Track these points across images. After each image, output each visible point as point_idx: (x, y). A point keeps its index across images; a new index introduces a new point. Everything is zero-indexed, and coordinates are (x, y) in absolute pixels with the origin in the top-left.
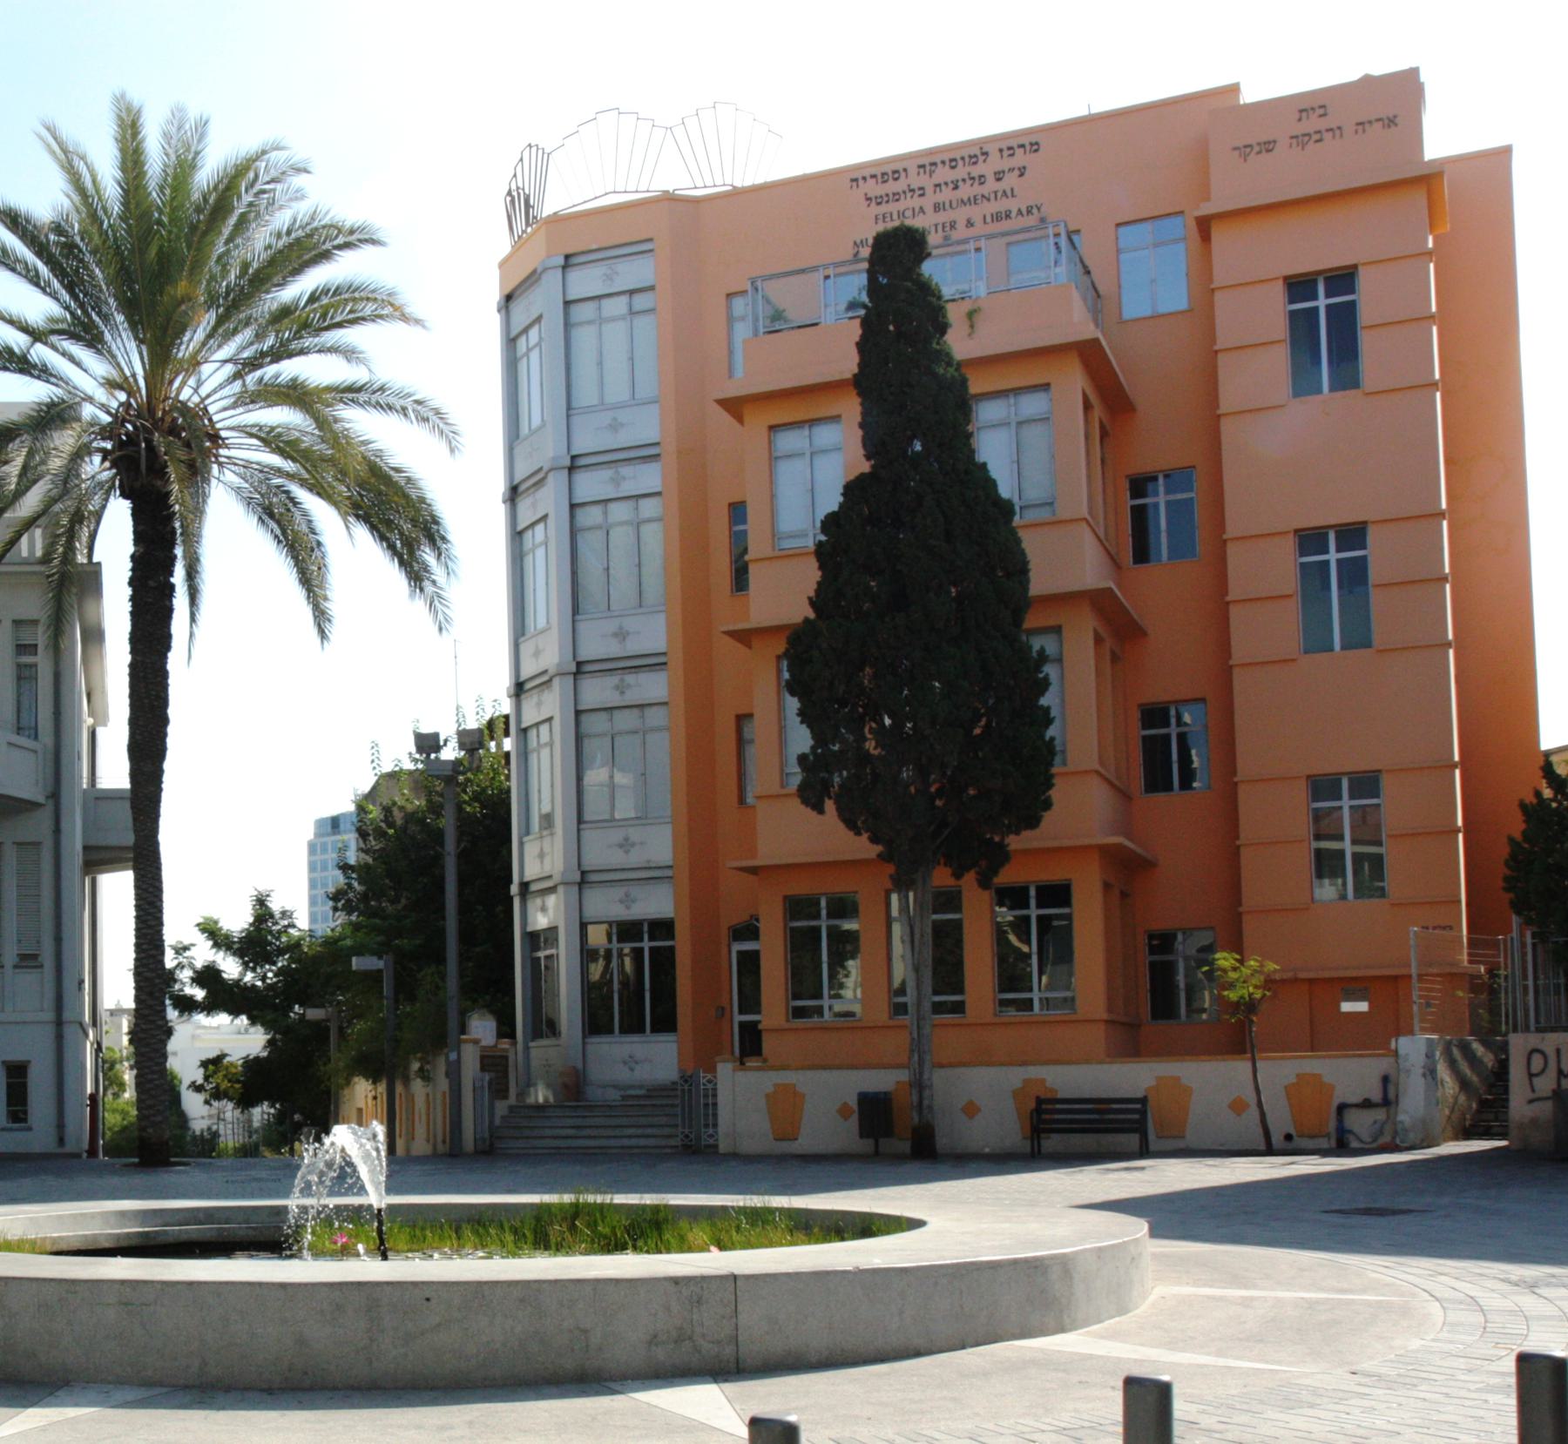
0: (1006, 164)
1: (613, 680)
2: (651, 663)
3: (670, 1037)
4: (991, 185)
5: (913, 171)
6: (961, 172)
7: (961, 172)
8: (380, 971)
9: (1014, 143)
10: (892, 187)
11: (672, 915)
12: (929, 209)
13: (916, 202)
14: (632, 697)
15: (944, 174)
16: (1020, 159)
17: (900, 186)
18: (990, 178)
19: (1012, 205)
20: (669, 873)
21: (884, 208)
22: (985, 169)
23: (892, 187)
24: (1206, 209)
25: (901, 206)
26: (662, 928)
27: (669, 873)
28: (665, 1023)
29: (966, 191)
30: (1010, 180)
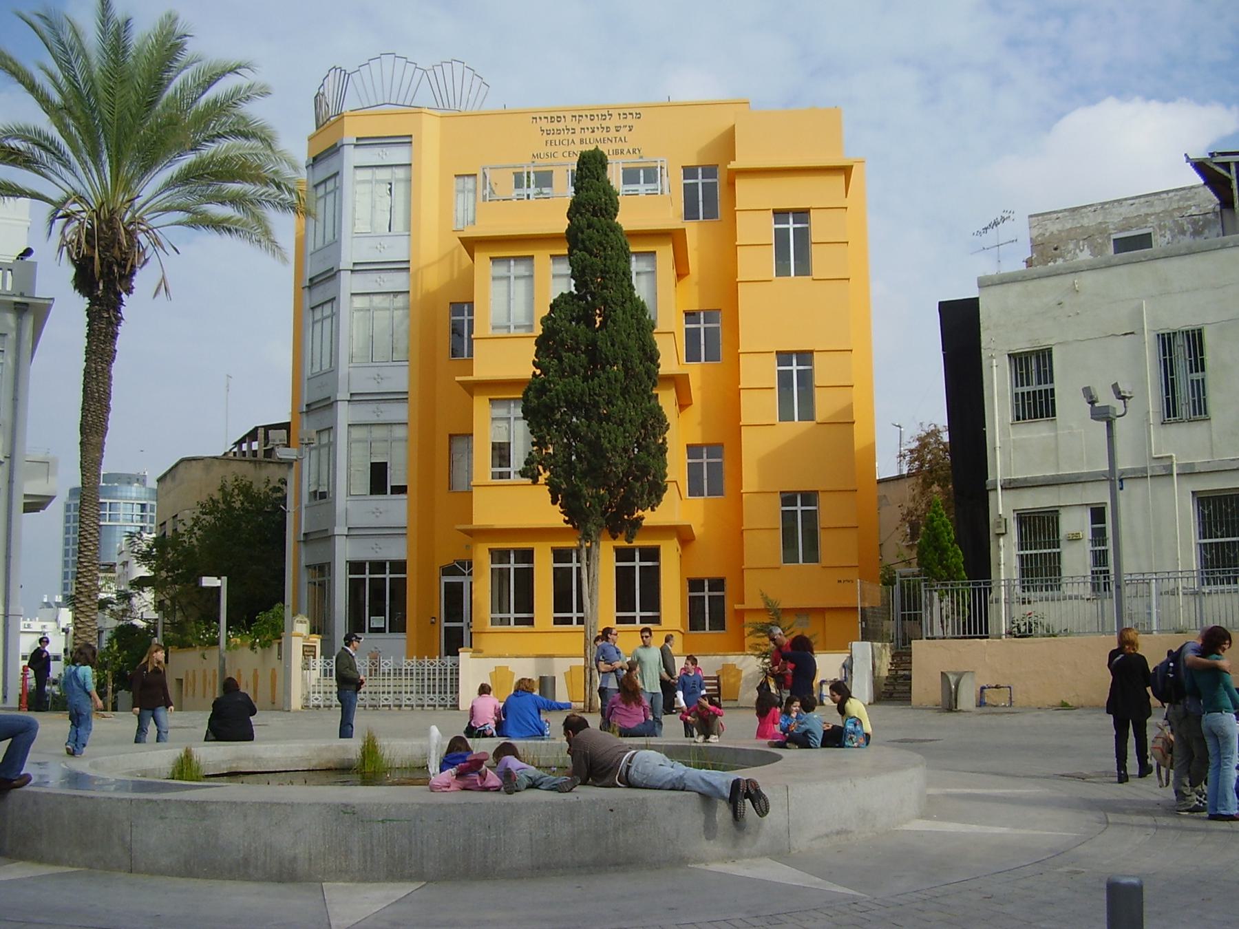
0: (622, 123)
1: (373, 406)
2: (399, 397)
3: (402, 635)
4: (613, 133)
5: (569, 118)
6: (596, 123)
7: (596, 123)
8: (218, 588)
9: (627, 111)
10: (556, 125)
11: (403, 558)
12: (577, 141)
13: (570, 137)
14: (382, 419)
15: (586, 123)
16: (630, 121)
17: (561, 126)
18: (613, 129)
19: (626, 147)
20: (404, 531)
21: (551, 137)
22: (611, 123)
23: (556, 125)
24: (733, 165)
25: (561, 137)
26: (399, 566)
27: (404, 531)
28: (398, 625)
29: (599, 134)
30: (624, 132)
